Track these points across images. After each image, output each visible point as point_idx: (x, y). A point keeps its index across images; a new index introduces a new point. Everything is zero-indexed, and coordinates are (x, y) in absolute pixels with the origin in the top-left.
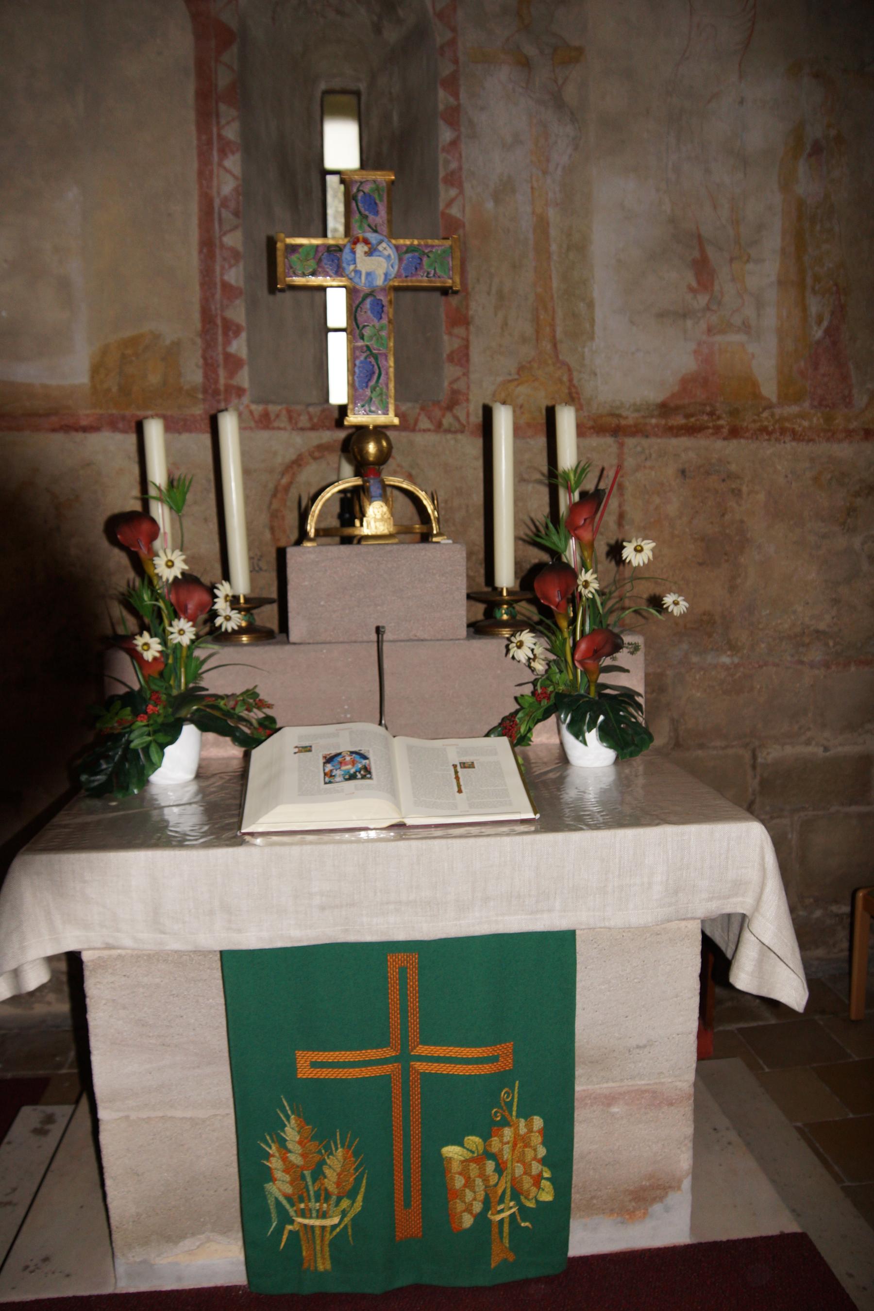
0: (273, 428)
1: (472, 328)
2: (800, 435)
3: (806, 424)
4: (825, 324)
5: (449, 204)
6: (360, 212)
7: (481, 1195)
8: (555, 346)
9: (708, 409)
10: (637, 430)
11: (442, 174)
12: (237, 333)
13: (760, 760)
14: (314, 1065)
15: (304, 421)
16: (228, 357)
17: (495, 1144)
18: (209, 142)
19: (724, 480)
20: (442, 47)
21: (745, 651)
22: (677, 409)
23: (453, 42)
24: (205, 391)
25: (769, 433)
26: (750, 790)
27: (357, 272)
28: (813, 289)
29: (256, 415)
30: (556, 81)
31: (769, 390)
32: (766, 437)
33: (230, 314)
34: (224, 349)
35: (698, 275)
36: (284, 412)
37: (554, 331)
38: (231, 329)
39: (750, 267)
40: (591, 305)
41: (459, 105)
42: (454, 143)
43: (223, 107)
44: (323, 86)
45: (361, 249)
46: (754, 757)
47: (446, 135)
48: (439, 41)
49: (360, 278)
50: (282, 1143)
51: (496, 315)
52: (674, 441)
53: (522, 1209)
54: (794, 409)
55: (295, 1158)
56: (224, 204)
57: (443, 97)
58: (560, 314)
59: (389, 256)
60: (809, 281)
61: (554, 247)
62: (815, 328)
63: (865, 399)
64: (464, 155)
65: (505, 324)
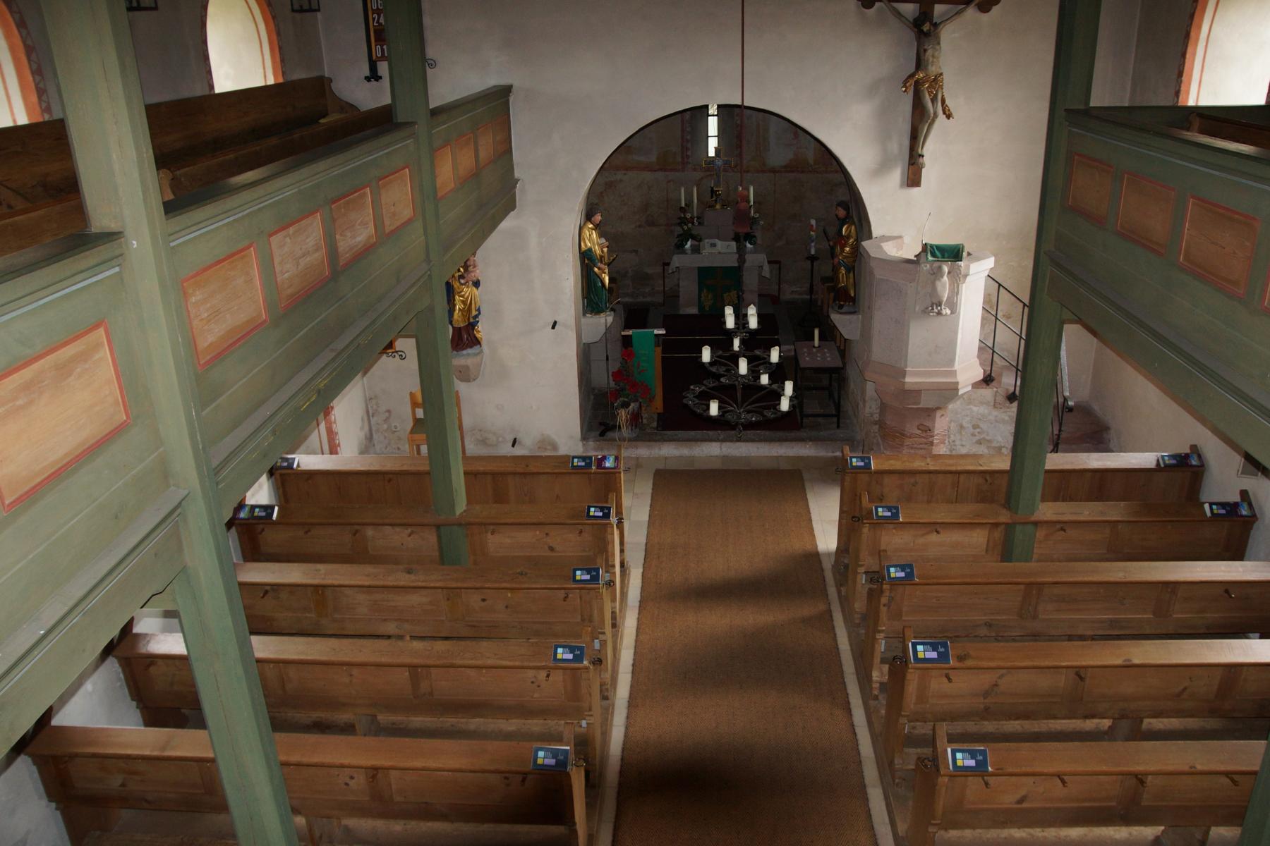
31: (811, 162)
38: (687, 149)
54: (817, 166)
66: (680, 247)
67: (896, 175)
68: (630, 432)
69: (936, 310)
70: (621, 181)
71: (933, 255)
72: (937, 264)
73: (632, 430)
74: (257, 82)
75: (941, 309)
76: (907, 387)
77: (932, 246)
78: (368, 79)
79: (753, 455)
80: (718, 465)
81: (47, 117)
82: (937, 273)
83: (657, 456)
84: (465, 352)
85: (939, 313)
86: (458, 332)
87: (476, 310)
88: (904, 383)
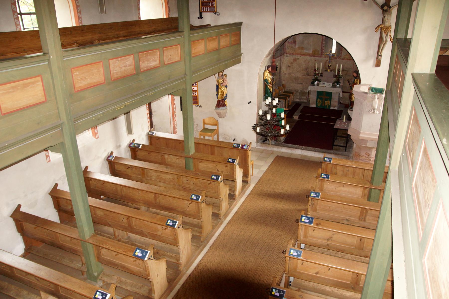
12: (324, 50)
38: (323, 50)
56: (324, 40)
66: (313, 84)
67: (372, 62)
68: (272, 142)
69: (372, 111)
70: (299, 59)
71: (372, 91)
72: (374, 95)
73: (273, 141)
74: (161, 17)
75: (375, 111)
76: (360, 138)
77: (372, 88)
78: (198, 18)
79: (312, 156)
80: (299, 157)
81: (80, 25)
82: (374, 98)
83: (280, 151)
84: (220, 108)
85: (374, 113)
86: (219, 102)
87: (225, 95)
88: (359, 136)
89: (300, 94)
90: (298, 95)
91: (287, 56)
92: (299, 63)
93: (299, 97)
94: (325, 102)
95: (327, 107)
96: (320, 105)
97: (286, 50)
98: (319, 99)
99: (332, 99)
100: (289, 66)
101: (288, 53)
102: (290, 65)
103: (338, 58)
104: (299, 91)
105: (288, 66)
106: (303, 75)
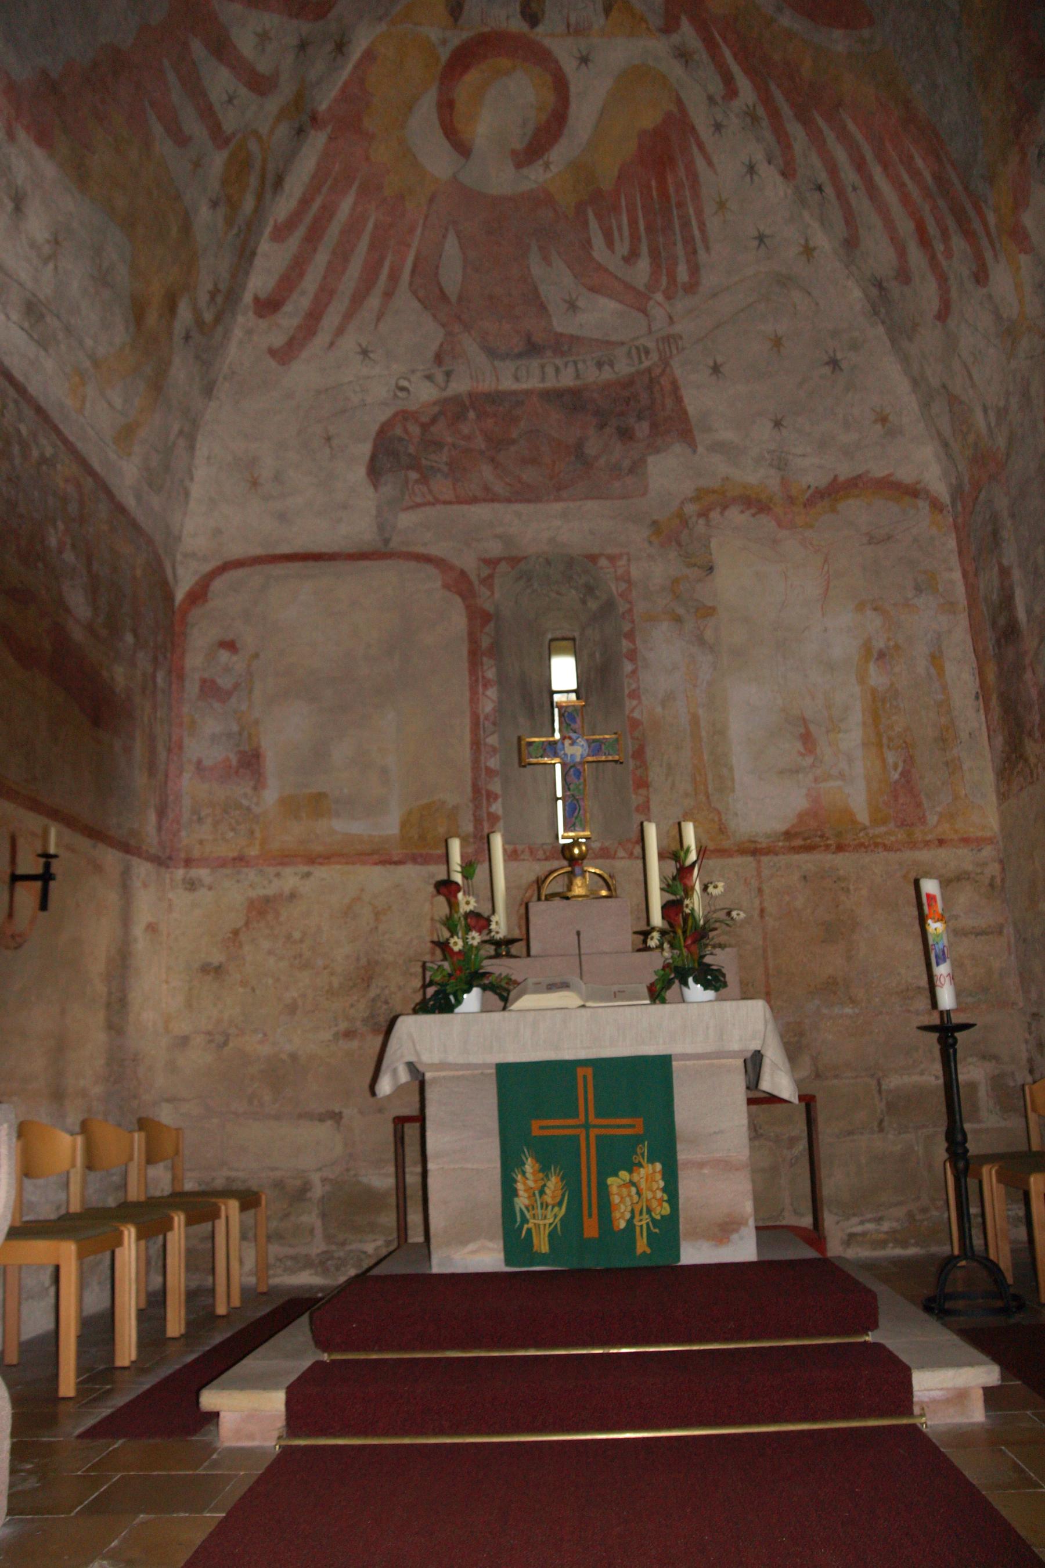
0: (520, 860)
1: (651, 789)
2: (890, 847)
3: (893, 838)
4: (900, 769)
5: (632, 710)
6: (566, 723)
7: (629, 1208)
8: (708, 798)
9: (819, 833)
10: (769, 851)
11: (627, 691)
12: (496, 797)
13: (884, 1087)
14: (542, 1128)
15: (540, 854)
16: (489, 814)
17: (635, 1178)
18: (477, 681)
19: (835, 882)
20: (623, 614)
21: (863, 1004)
22: (796, 835)
23: (630, 610)
24: (475, 837)
25: (866, 847)
26: (879, 1111)
27: (565, 754)
28: (889, 747)
29: (509, 852)
30: (699, 628)
31: (863, 817)
32: (865, 850)
33: (491, 787)
34: (488, 808)
35: (804, 744)
36: (527, 849)
37: (707, 788)
38: (491, 796)
39: (841, 735)
40: (731, 769)
41: (636, 648)
42: (634, 672)
43: (485, 659)
44: (550, 636)
45: (567, 742)
46: (879, 1084)
47: (628, 667)
48: (621, 610)
49: (567, 758)
50: (524, 1173)
51: (666, 780)
52: (796, 857)
53: (653, 1220)
54: (883, 829)
55: (531, 1184)
56: (486, 718)
57: (625, 644)
58: (710, 777)
59: (583, 746)
60: (885, 741)
61: (704, 734)
62: (893, 773)
63: (936, 818)
64: (640, 678)
65: (673, 785)
70: (293, 896)
89: (323, 1215)
90: (312, 1231)
91: (192, 885)
92: (297, 935)
93: (317, 1247)
94: (604, 1192)
95: (642, 1245)
96: (552, 1235)
97: (183, 834)
98: (530, 1166)
99: (679, 1147)
100: (216, 971)
101: (196, 854)
102: (217, 957)
103: (621, 853)
104: (318, 1191)
105: (206, 969)
106: (336, 1035)
